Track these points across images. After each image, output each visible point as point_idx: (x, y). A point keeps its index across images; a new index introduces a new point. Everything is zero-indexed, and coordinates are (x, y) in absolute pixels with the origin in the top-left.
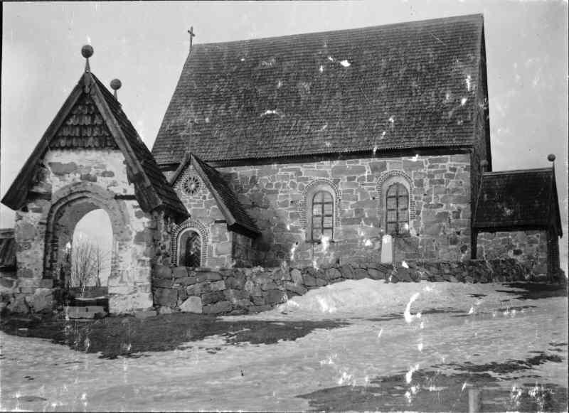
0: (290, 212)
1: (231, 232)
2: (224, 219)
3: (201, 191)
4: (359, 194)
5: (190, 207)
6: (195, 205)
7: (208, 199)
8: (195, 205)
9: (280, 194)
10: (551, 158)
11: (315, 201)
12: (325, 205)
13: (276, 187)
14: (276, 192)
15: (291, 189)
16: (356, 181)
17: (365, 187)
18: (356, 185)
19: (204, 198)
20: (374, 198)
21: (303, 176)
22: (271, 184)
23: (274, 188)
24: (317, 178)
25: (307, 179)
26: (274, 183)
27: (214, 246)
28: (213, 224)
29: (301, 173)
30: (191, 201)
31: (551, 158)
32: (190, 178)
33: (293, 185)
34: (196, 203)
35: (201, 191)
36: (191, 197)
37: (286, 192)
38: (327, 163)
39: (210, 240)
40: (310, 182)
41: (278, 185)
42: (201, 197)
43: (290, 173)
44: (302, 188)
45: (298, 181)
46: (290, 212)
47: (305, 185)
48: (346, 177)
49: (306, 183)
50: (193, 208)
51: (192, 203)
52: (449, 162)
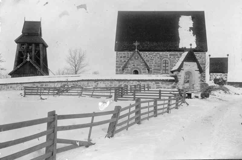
9: (154, 60)
10: (228, 55)
18: (176, 59)
29: (160, 55)
31: (228, 55)
33: (158, 58)
50: (137, 64)
52: (200, 54)
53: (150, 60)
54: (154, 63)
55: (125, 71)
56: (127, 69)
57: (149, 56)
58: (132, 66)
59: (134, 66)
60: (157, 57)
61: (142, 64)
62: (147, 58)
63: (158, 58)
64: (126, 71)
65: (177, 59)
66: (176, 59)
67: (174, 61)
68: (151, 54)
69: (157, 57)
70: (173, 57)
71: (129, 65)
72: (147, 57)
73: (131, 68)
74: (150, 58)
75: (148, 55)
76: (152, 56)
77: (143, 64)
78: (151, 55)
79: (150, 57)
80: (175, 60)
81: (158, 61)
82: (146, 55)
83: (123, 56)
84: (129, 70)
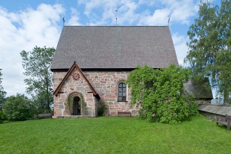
0: (111, 90)
1: (94, 97)
2: (91, 91)
3: (81, 79)
5: (75, 85)
6: (78, 85)
7: (84, 83)
8: (78, 85)
9: (107, 83)
11: (123, 84)
12: (123, 88)
13: (105, 80)
14: (106, 82)
15: (111, 81)
19: (82, 82)
21: (116, 77)
22: (103, 79)
23: (104, 81)
24: (121, 78)
25: (117, 78)
26: (104, 79)
27: (87, 102)
28: (87, 93)
29: (115, 76)
30: (76, 83)
32: (75, 74)
33: (112, 80)
34: (79, 84)
35: (81, 79)
36: (76, 82)
38: (125, 72)
40: (118, 79)
43: (111, 76)
44: (115, 81)
45: (114, 78)
46: (111, 90)
47: (117, 80)
49: (117, 80)
51: (77, 84)
53: (101, 83)
54: (106, 87)
56: (61, 94)
57: (99, 77)
59: (73, 90)
60: (110, 79)
61: (85, 87)
62: (97, 80)
63: (112, 80)
64: (60, 98)
68: (102, 75)
69: (110, 79)
72: (97, 79)
73: (68, 93)
74: (101, 80)
75: (98, 75)
76: (104, 77)
77: (87, 86)
78: (102, 77)
79: (101, 79)
81: (112, 84)
82: (95, 76)
84: (65, 96)
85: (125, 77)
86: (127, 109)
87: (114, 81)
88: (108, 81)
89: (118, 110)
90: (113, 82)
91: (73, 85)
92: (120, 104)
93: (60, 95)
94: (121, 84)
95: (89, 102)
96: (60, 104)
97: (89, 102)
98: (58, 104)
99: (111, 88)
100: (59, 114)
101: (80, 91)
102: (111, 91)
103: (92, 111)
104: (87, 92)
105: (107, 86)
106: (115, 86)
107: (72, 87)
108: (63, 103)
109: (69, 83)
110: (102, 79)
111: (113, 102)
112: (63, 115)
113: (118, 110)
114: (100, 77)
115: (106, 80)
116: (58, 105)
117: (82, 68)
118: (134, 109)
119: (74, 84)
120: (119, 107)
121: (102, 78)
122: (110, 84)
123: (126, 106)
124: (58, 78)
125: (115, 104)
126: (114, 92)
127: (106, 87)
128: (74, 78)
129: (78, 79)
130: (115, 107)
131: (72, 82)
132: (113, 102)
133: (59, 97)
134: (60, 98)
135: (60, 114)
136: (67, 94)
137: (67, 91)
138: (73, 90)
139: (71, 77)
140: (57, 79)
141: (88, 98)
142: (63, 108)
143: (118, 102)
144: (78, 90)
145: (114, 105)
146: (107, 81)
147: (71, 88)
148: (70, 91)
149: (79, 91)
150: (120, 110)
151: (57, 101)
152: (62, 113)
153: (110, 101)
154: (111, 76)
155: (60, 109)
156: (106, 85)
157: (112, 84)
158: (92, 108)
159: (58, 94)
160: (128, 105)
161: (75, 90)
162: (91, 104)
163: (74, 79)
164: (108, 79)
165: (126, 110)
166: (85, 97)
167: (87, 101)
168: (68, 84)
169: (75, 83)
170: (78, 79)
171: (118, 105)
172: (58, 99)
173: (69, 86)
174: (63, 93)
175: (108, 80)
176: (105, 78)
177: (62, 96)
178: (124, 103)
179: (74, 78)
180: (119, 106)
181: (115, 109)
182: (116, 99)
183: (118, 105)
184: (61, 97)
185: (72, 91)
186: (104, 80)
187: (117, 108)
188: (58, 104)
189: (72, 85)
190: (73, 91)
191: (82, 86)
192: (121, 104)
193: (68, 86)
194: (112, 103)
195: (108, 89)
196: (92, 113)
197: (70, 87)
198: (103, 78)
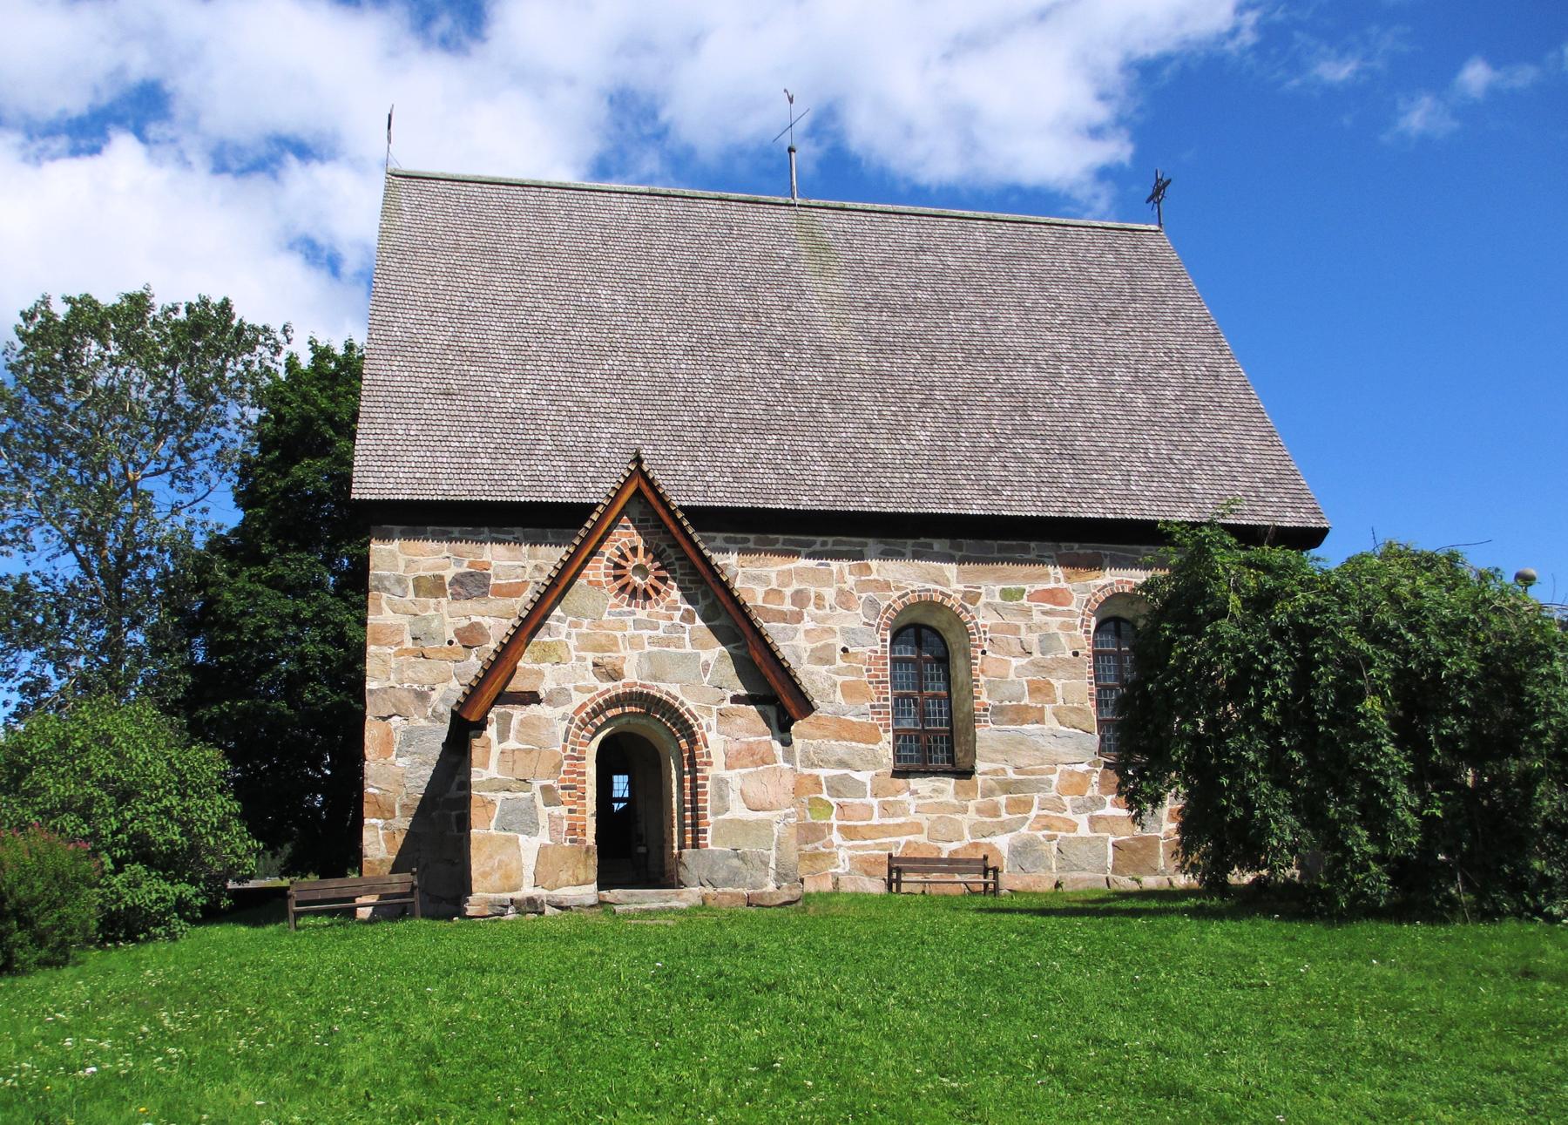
0: (839, 679)
4: (1033, 639)
5: (634, 643)
9: (807, 624)
13: (793, 603)
14: (798, 618)
16: (1024, 601)
17: (1055, 622)
18: (1027, 613)
20: (1076, 654)
23: (787, 606)
24: (917, 585)
25: (887, 586)
26: (788, 591)
28: (727, 704)
33: (845, 600)
34: (660, 633)
36: (641, 614)
37: (824, 619)
39: (718, 758)
41: (800, 598)
42: (678, 615)
46: (839, 679)
47: (884, 604)
48: (998, 588)
50: (648, 648)
51: (646, 633)
54: (805, 656)
55: (496, 749)
56: (518, 713)
58: (592, 680)
64: (512, 744)
65: (1037, 617)
66: (1027, 613)
67: (1016, 630)
69: (829, 594)
70: (998, 588)
71: (546, 667)
73: (578, 699)
80: (1021, 622)
83: (449, 575)
85: (947, 583)
86: (974, 830)
87: (860, 611)
88: (819, 606)
89: (903, 840)
90: (855, 619)
91: (619, 634)
92: (914, 793)
93: (505, 721)
94: (911, 631)
95: (743, 777)
96: (507, 795)
97: (743, 777)
98: (490, 795)
99: (840, 663)
100: (495, 879)
101: (675, 690)
102: (843, 685)
103: (773, 853)
104: (729, 694)
105: (809, 646)
106: (875, 644)
107: (607, 658)
108: (537, 785)
109: (586, 622)
110: (767, 593)
111: (864, 776)
112: (527, 891)
113: (903, 840)
114: (756, 578)
115: (800, 598)
116: (492, 802)
117: (697, 501)
118: (1024, 830)
119: (624, 627)
120: (913, 817)
121: (767, 581)
122: (831, 631)
123: (965, 810)
124: (411, 576)
125: (876, 795)
126: (865, 695)
127: (805, 656)
128: (620, 582)
129: (658, 592)
130: (875, 821)
131: (606, 616)
132: (864, 776)
133: (503, 735)
134: (512, 744)
135: (507, 877)
136: (569, 709)
137: (570, 686)
138: (614, 675)
139: (598, 570)
140: (400, 581)
141: (736, 746)
142: (532, 828)
143: (901, 782)
144: (655, 678)
145: (875, 802)
146: (811, 608)
147: (595, 665)
148: (590, 691)
149: (664, 686)
150: (922, 839)
151: (485, 765)
152: (520, 868)
153: (842, 763)
154: (841, 571)
155: (508, 840)
156: (801, 635)
157: (844, 631)
158: (769, 824)
159: (497, 709)
160: (979, 799)
161: (633, 677)
162: (753, 789)
163: (623, 589)
164: (812, 590)
165: (968, 839)
166: (712, 737)
167: (728, 767)
168: (574, 631)
169: (629, 620)
170: (658, 592)
171: (905, 796)
172: (487, 747)
173: (587, 643)
174: (532, 698)
175: (819, 597)
176: (795, 586)
177: (522, 723)
178: (949, 784)
179: (620, 582)
180: (905, 812)
181: (883, 830)
182: (885, 748)
183: (905, 796)
184: (512, 735)
185: (610, 685)
186: (788, 600)
187: (891, 821)
188: (490, 795)
189: (603, 640)
190: (618, 688)
191: (688, 649)
192: (922, 792)
193: (573, 642)
194: (858, 788)
195: (823, 669)
196: (772, 864)
197: (591, 657)
198: (774, 586)
